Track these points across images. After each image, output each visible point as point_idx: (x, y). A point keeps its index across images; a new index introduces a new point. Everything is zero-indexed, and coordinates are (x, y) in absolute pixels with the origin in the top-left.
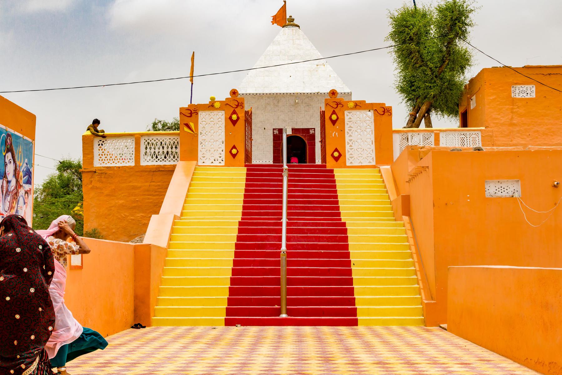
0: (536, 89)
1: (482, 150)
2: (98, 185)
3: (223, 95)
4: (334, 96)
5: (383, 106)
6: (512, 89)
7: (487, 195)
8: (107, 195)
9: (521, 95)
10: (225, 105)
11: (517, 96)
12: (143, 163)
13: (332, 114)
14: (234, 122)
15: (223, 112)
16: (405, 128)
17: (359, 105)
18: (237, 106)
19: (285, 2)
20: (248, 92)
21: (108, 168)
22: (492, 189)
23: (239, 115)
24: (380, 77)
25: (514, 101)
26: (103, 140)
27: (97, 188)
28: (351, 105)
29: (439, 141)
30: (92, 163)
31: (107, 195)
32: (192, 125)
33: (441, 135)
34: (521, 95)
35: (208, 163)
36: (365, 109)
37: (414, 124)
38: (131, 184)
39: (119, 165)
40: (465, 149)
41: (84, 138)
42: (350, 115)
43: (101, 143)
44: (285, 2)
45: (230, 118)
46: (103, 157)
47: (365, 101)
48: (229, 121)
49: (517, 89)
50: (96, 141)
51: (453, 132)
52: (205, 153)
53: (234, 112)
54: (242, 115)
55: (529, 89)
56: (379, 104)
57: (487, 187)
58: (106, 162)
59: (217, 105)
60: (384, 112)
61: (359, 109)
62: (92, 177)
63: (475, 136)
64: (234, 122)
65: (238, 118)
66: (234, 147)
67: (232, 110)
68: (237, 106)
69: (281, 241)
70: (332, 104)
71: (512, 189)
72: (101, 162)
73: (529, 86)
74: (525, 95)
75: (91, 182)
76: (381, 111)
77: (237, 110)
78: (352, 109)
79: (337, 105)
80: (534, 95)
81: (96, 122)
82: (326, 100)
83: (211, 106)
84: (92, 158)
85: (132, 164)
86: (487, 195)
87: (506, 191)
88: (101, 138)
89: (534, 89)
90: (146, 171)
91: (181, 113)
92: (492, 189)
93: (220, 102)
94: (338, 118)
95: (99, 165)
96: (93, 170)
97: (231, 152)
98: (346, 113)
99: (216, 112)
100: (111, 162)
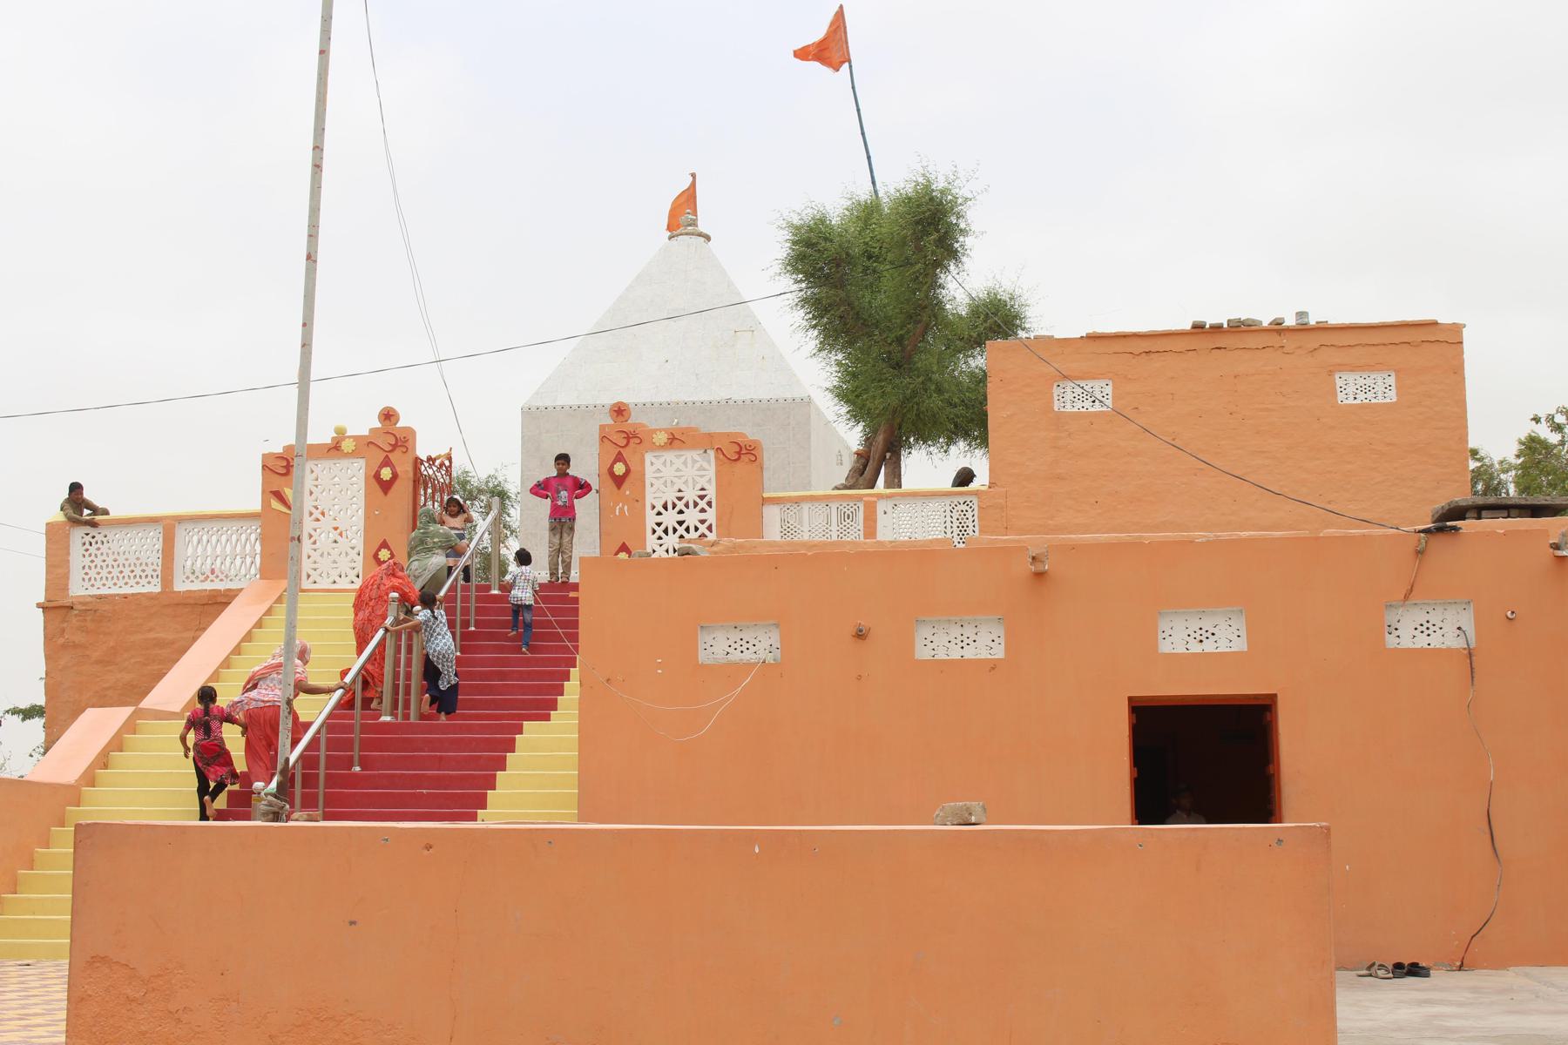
0: (1398, 380)
1: (695, 553)
2: (79, 638)
3: (364, 423)
4: (620, 418)
5: (739, 440)
6: (1056, 391)
7: (703, 657)
8: (98, 662)
9: (1079, 405)
10: (366, 444)
11: (1069, 408)
12: (181, 586)
13: (615, 462)
14: (386, 486)
15: (362, 462)
16: (837, 488)
17: (676, 440)
18: (394, 447)
19: (693, 176)
20: (559, 403)
21: (100, 597)
22: (717, 647)
23: (399, 470)
24: (794, 366)
25: (1060, 420)
26: (93, 531)
27: (75, 646)
28: (661, 438)
29: (875, 521)
30: (65, 588)
31: (98, 662)
32: (289, 493)
33: (180, 533)
34: (1079, 405)
35: (325, 584)
36: (693, 447)
37: (861, 480)
38: (152, 635)
39: (127, 590)
40: (833, 543)
41: (51, 529)
42: (658, 464)
43: (88, 539)
44: (693, 176)
45: (377, 476)
46: (92, 573)
47: (695, 430)
48: (373, 481)
49: (1069, 390)
50: (78, 534)
51: (235, 525)
52: (319, 559)
53: (387, 463)
54: (405, 469)
55: (1380, 381)
56: (728, 435)
57: (1164, 624)
58: (98, 584)
59: (348, 446)
60: (739, 453)
61: (680, 449)
62: (64, 621)
63: (964, 507)
64: (386, 486)
65: (395, 476)
66: (384, 545)
67: (381, 456)
68: (394, 447)
69: (303, 775)
70: (615, 438)
71: (765, 644)
72: (87, 585)
73: (1378, 376)
74: (1088, 404)
75: (63, 630)
76: (731, 451)
77: (392, 457)
78: (661, 447)
79: (628, 439)
80: (1392, 396)
81: (76, 488)
82: (602, 427)
83: (334, 449)
84: (66, 576)
85: (155, 588)
86: (703, 657)
87: (752, 649)
88: (88, 529)
89: (1109, 390)
90: (186, 605)
91: (264, 467)
92: (717, 647)
93: (356, 438)
94: (628, 472)
95: (83, 593)
96: (67, 602)
97: (376, 556)
98: (649, 457)
99: (344, 463)
100: (110, 583)
